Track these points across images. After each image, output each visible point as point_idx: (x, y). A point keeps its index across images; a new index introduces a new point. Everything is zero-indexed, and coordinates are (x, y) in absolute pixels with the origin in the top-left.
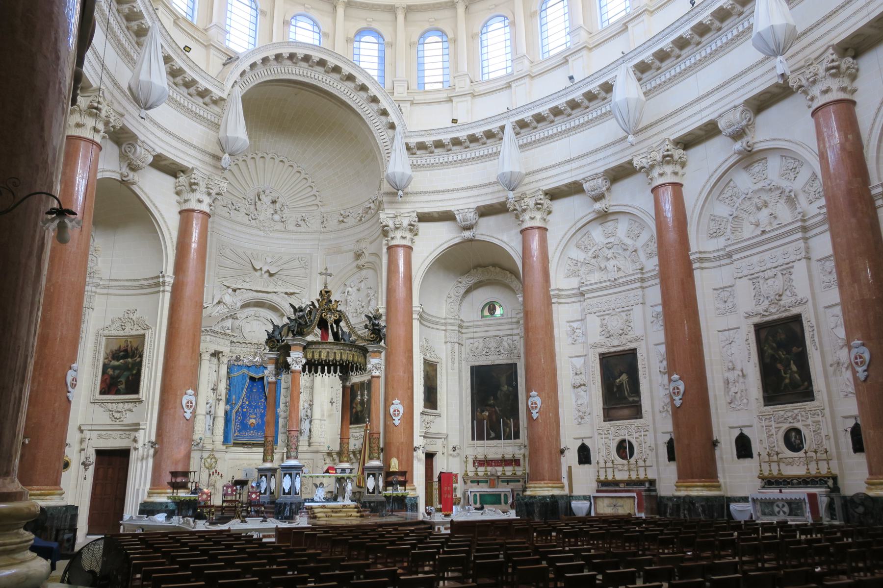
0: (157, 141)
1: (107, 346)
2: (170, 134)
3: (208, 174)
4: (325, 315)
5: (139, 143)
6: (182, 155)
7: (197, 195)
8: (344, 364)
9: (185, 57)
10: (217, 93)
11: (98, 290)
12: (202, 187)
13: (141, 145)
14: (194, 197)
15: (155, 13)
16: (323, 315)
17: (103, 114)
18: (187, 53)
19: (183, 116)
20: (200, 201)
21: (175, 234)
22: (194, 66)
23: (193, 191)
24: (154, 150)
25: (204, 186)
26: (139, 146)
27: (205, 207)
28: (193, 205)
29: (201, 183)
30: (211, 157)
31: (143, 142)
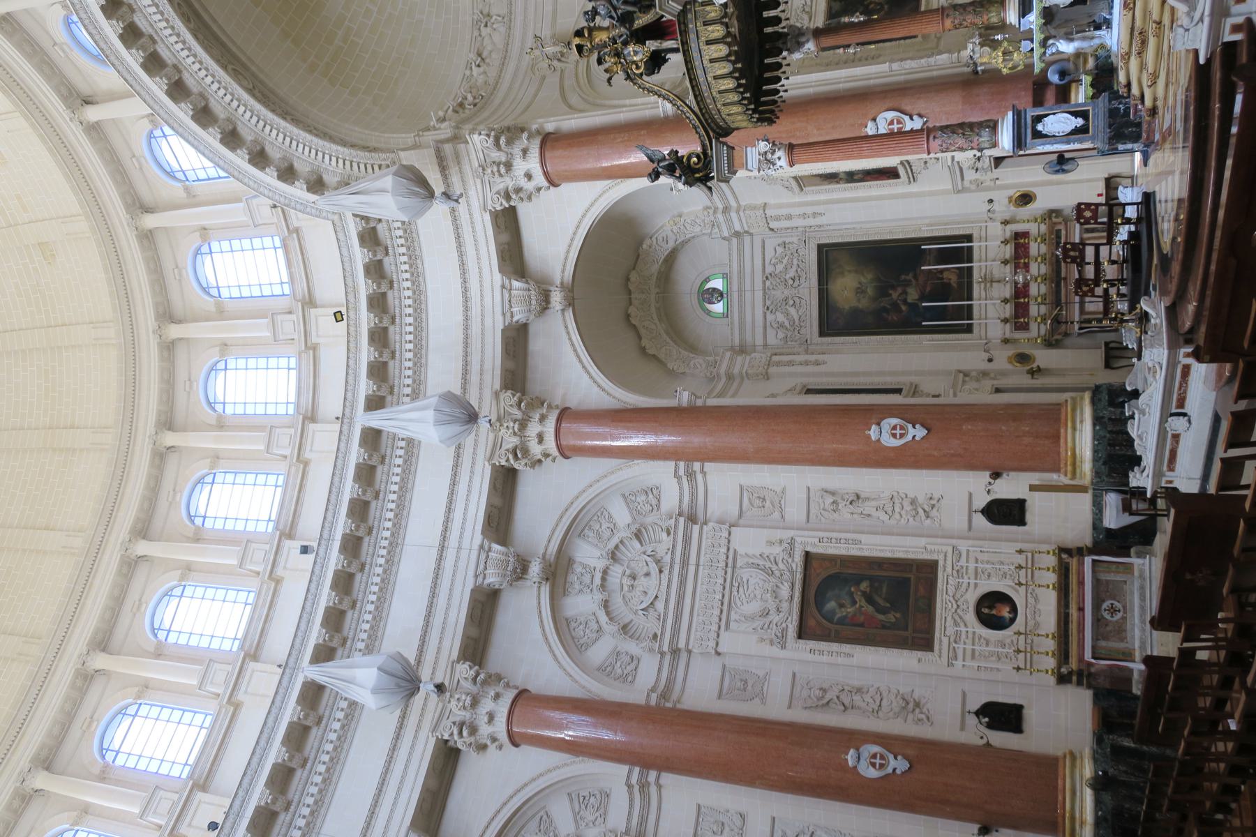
0: (487, 284)
1: (816, 185)
2: (463, 264)
3: (478, 181)
4: (638, 68)
5: (508, 320)
6: (479, 228)
7: (523, 182)
8: (739, 65)
9: (352, 314)
10: (353, 228)
11: (733, 204)
12: (509, 183)
13: (509, 314)
14: (529, 186)
15: (343, 414)
16: (636, 72)
17: (512, 442)
18: (344, 311)
19: (422, 239)
20: (529, 176)
21: (601, 185)
22: (350, 289)
23: (518, 190)
24: (503, 287)
25: (497, 179)
26: (512, 317)
27: (533, 164)
28: (540, 179)
29: (501, 186)
30: (447, 172)
31: (504, 314)
